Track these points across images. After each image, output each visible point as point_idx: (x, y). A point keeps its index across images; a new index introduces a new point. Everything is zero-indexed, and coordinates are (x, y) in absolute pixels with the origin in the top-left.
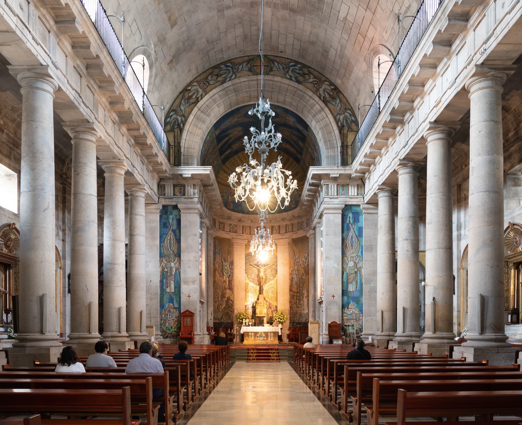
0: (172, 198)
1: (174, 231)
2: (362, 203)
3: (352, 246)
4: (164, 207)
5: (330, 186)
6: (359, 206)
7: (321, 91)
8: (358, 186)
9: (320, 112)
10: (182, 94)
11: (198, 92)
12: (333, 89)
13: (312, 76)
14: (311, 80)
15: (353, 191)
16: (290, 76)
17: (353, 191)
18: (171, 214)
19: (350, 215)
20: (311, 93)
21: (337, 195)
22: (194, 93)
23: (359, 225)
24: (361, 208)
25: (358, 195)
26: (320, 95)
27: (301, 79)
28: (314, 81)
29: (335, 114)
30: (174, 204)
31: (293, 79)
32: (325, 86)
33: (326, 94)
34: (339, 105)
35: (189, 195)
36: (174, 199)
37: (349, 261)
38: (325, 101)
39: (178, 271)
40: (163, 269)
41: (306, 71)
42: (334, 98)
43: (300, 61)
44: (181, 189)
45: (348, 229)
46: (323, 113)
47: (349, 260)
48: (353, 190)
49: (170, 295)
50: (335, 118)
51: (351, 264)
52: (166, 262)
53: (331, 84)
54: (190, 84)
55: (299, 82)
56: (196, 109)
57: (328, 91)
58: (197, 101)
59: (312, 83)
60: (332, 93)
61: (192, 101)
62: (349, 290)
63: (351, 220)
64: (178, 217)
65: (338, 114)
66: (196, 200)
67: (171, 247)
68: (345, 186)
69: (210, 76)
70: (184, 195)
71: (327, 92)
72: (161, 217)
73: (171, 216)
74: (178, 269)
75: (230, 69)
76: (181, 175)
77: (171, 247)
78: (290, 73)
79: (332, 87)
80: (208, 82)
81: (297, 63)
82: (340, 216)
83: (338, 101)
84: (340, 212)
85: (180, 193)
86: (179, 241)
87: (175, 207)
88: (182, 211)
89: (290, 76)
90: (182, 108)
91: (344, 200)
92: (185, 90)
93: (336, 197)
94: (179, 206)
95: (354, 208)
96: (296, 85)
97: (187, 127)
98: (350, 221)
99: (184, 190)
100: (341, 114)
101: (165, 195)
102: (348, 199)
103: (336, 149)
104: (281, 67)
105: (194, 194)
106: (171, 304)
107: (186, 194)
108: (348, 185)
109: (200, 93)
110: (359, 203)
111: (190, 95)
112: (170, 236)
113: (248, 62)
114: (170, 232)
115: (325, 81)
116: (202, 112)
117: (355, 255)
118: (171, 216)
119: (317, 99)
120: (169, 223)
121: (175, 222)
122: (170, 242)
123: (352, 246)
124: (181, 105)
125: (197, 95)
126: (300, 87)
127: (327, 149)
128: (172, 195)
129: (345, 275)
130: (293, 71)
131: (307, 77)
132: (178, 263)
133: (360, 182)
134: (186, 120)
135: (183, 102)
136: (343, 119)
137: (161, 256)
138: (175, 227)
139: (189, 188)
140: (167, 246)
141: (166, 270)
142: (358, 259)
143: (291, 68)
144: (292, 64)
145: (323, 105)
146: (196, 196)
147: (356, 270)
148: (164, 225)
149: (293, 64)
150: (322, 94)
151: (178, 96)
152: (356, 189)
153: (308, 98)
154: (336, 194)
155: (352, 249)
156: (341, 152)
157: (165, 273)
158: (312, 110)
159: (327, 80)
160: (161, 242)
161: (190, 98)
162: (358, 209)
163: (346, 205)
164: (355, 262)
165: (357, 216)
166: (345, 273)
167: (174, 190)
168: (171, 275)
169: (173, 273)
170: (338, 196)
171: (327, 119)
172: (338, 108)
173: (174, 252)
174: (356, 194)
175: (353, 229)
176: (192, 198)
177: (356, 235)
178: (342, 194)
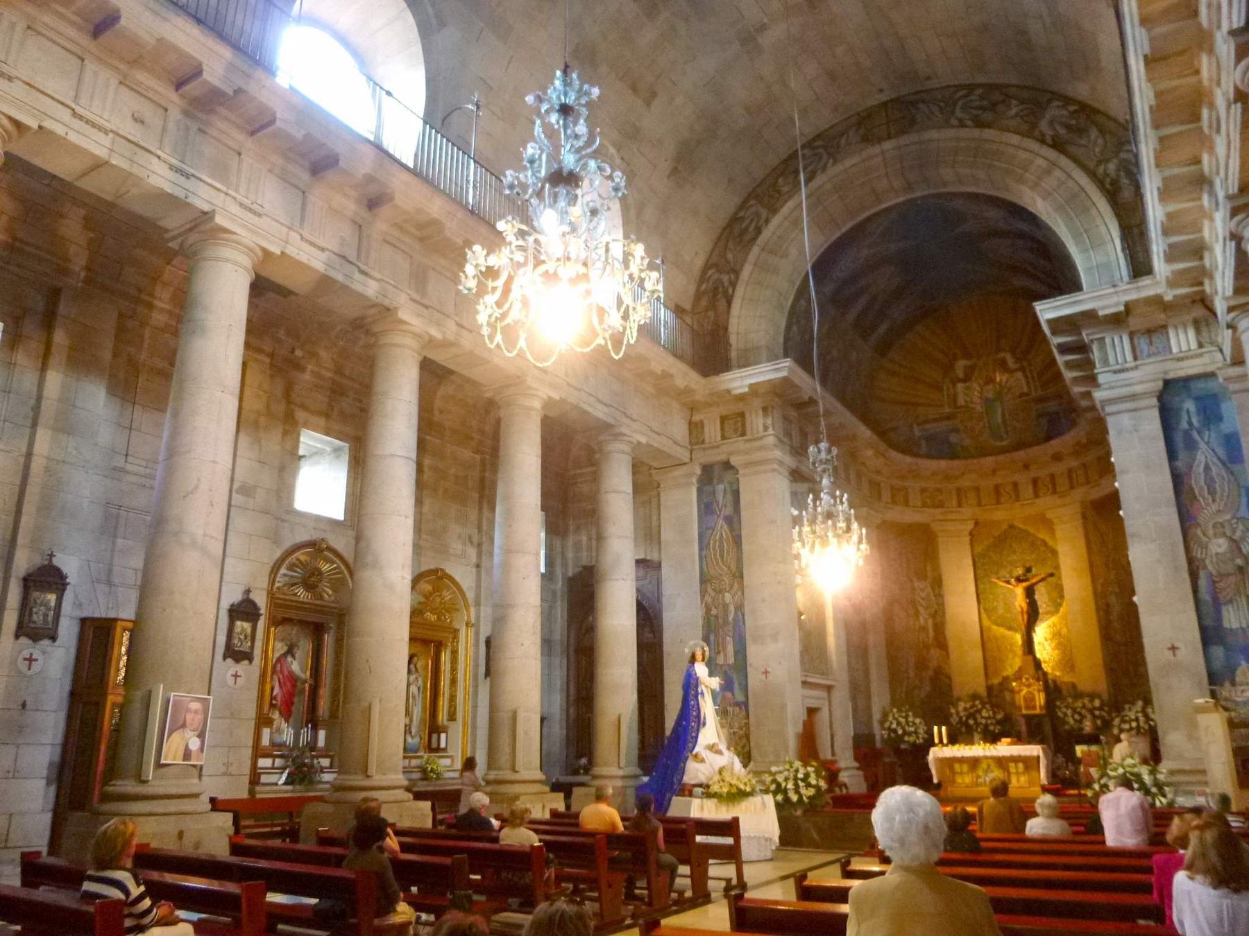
0: (718, 447)
1: (728, 520)
2: (1220, 365)
3: (1212, 492)
4: (707, 469)
5: (1108, 341)
6: (1212, 375)
7: (1044, 126)
8: (1197, 324)
9: (1048, 172)
10: (727, 231)
11: (758, 215)
12: (1076, 111)
13: (1014, 102)
14: (1013, 112)
15: (1182, 340)
16: (960, 120)
17: (1182, 340)
18: (721, 481)
19: (1190, 405)
20: (1015, 139)
21: (1135, 358)
22: (752, 220)
23: (1226, 427)
24: (1221, 380)
25: (1201, 345)
26: (1043, 135)
27: (987, 116)
28: (1022, 111)
29: (1092, 165)
30: (723, 457)
31: (969, 123)
32: (1055, 111)
33: (1058, 128)
34: (1100, 141)
35: (755, 431)
36: (724, 448)
37: (1212, 536)
38: (1058, 145)
39: (739, 613)
40: (708, 609)
41: (997, 96)
42: (1080, 131)
43: (981, 79)
44: (736, 423)
45: (1191, 446)
46: (1057, 173)
47: (1211, 532)
48: (1182, 337)
49: (726, 672)
50: (1092, 175)
51: (1219, 546)
52: (713, 594)
53: (1067, 100)
54: (743, 206)
55: (981, 125)
56: (755, 250)
57: (1064, 120)
58: (758, 231)
59: (1016, 115)
60: (1074, 122)
61: (747, 237)
62: (1226, 624)
63: (1195, 421)
64: (735, 487)
65: (1099, 162)
66: (771, 440)
67: (722, 557)
68: (1155, 331)
69: (780, 180)
70: (743, 434)
71: (1061, 124)
72: (699, 491)
73: (721, 487)
74: (740, 607)
75: (821, 150)
76: (728, 391)
77: (722, 557)
78: (958, 113)
79: (1072, 108)
80: (779, 192)
81: (971, 88)
82: (1155, 414)
83: (1094, 133)
84: (1154, 401)
85: (736, 430)
86: (737, 541)
87: (727, 466)
88: (741, 472)
89: (960, 120)
90: (730, 256)
91: (1159, 368)
92: (735, 220)
93: (1133, 364)
94: (734, 461)
95: (1200, 385)
96: (976, 133)
97: (740, 290)
98: (1190, 423)
99: (744, 425)
100: (1108, 161)
101: (703, 442)
102: (1170, 365)
103: (1110, 246)
104: (936, 109)
105: (766, 428)
106: (729, 695)
107: (748, 433)
108: (1165, 327)
109: (764, 217)
110: (1209, 369)
111: (744, 225)
112: (721, 527)
113: (859, 125)
114: (721, 522)
115: (1049, 101)
116: (771, 252)
117: (1228, 517)
118: (721, 487)
119: (1035, 146)
120: (717, 502)
121: (729, 496)
122: (719, 546)
123: (1212, 492)
124: (728, 252)
125: (758, 222)
126: (988, 133)
127: (1084, 251)
128: (719, 438)
129: (1203, 582)
130: (964, 108)
131: (1001, 108)
132: (739, 593)
133: (1199, 312)
134: (737, 278)
135: (731, 245)
136: (1118, 170)
137: (704, 580)
138: (729, 511)
139: (754, 416)
140: (715, 555)
141: (714, 611)
142: (1241, 527)
143: (960, 103)
144: (961, 93)
145: (1052, 154)
146: (771, 431)
147: (1239, 561)
148: (706, 509)
149: (965, 92)
150: (1049, 133)
151: (719, 239)
152: (1191, 333)
153: (1011, 151)
154: (1129, 357)
155: (1214, 501)
156: (1123, 250)
157: (712, 618)
158: (1027, 175)
159: (1056, 95)
160: (701, 549)
161: (743, 232)
162: (1211, 385)
163: (1167, 383)
164: (1232, 540)
165: (1210, 409)
166: (1202, 574)
167: (722, 429)
168: (726, 622)
169: (731, 619)
170: (1138, 362)
171: (1071, 183)
172: (1097, 150)
173: (729, 568)
174: (1194, 345)
175: (1207, 443)
176: (761, 438)
177: (1219, 459)
178: (1149, 356)
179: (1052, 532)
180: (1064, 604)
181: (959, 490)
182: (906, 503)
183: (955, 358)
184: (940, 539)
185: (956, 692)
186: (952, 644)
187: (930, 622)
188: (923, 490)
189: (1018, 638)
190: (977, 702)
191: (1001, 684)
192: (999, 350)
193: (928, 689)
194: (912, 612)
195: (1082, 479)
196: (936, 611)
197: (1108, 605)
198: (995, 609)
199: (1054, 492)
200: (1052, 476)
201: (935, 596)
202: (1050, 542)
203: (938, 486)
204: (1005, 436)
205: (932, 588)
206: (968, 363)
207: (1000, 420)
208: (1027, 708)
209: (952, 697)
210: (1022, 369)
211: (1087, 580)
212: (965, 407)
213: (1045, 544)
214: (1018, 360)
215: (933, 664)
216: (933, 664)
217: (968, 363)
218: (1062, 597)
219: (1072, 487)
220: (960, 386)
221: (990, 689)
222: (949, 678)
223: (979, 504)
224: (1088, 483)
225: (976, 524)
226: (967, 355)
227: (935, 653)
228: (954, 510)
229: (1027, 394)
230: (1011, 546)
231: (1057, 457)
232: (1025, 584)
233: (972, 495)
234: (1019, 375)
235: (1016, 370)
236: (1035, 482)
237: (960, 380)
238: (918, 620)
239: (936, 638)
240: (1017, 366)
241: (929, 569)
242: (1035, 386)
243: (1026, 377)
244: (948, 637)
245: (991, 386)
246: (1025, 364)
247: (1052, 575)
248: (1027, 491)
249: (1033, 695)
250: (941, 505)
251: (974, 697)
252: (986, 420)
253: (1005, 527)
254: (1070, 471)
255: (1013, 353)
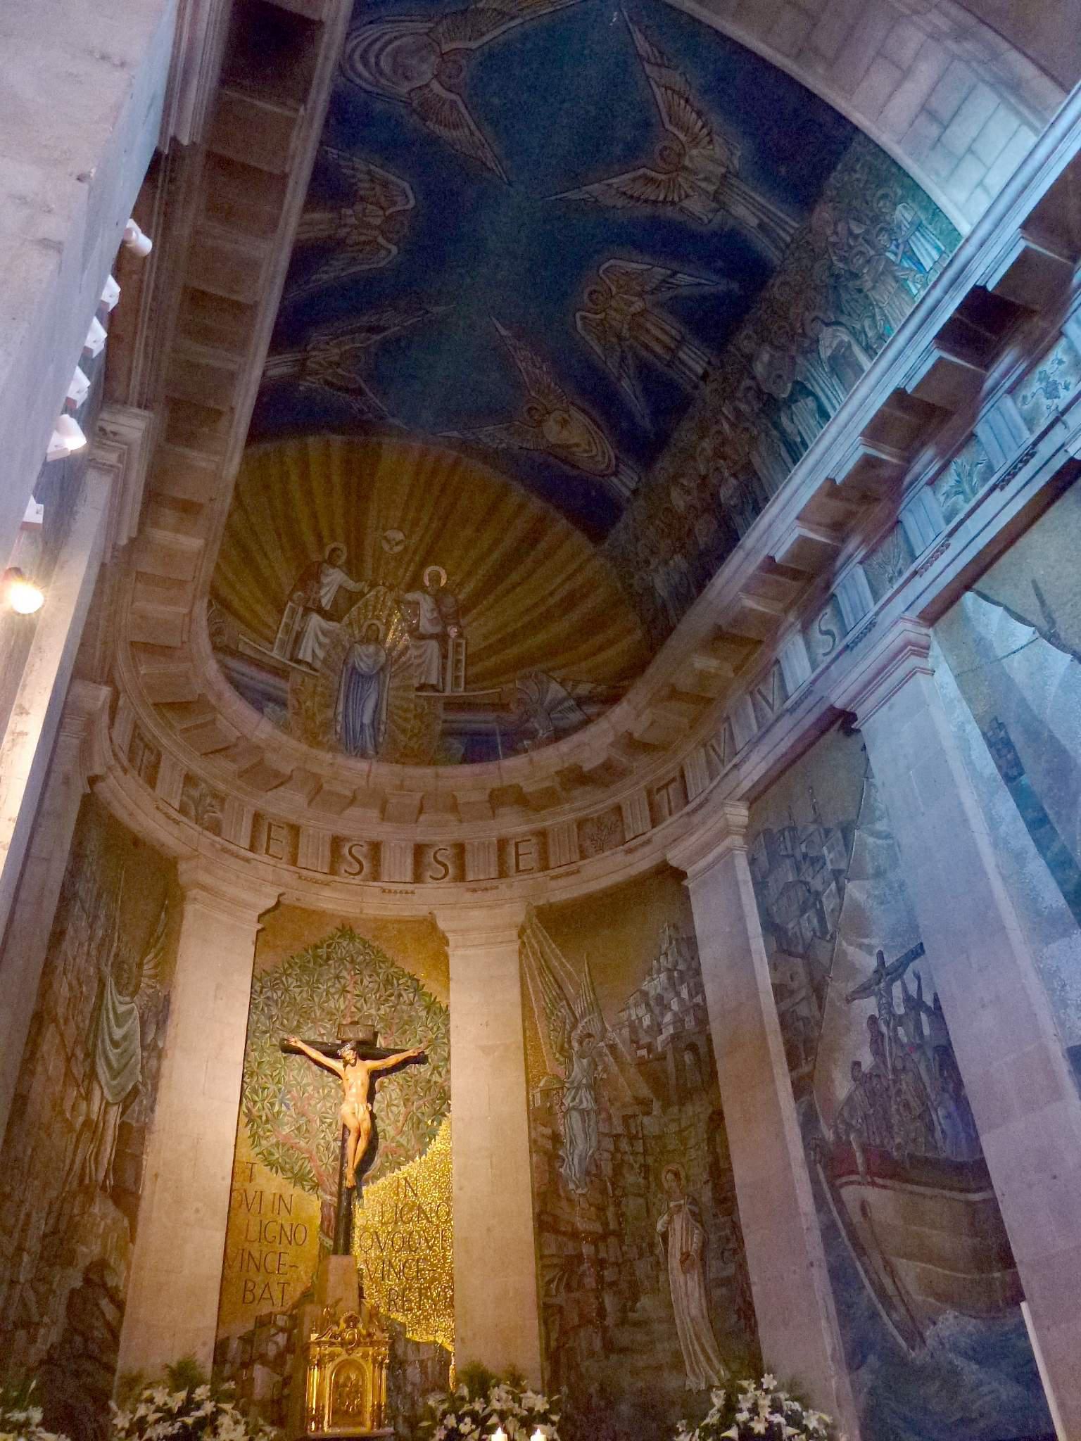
179: (440, 961)
180: (443, 1130)
181: (257, 817)
182: (152, 782)
183: (331, 562)
184: (190, 909)
185: (125, 1362)
186: (153, 1198)
187: (114, 1115)
188: (190, 780)
189: (312, 1206)
190: (201, 1392)
191: (247, 1340)
192: (415, 583)
193: (55, 1336)
194: (78, 1070)
195: (530, 859)
196: (135, 1092)
197: (556, 1138)
198: (274, 1118)
199: (461, 877)
200: (460, 849)
201: (144, 1047)
202: (431, 986)
203: (221, 787)
204: (371, 752)
205: (143, 1023)
206: (351, 585)
207: (367, 719)
208: (339, 1414)
209: (110, 1369)
210: (442, 638)
211: (515, 1076)
212: (309, 665)
213: (417, 989)
214: (444, 619)
215: (89, 1251)
216: (89, 1251)
217: (351, 585)
218: (439, 1115)
219: (502, 874)
220: (315, 619)
221: (221, 1348)
222: (120, 1306)
223: (294, 861)
224: (545, 867)
225: (278, 903)
226: (353, 568)
227: (102, 1211)
228: (244, 853)
229: (434, 688)
230: (338, 977)
231: (498, 799)
232: (371, 1064)
233: (283, 835)
234: (433, 645)
235: (432, 637)
236: (419, 851)
237: (320, 611)
238: (88, 1097)
239: (116, 1167)
240: (437, 629)
241: (148, 969)
242: (457, 678)
243: (445, 657)
244: (147, 1174)
245: (372, 649)
246: (453, 631)
247: (420, 1059)
248: (398, 864)
249: (360, 1370)
250: (216, 828)
251: (182, 1376)
252: (341, 708)
253: (330, 930)
254: (502, 844)
255: (438, 602)
